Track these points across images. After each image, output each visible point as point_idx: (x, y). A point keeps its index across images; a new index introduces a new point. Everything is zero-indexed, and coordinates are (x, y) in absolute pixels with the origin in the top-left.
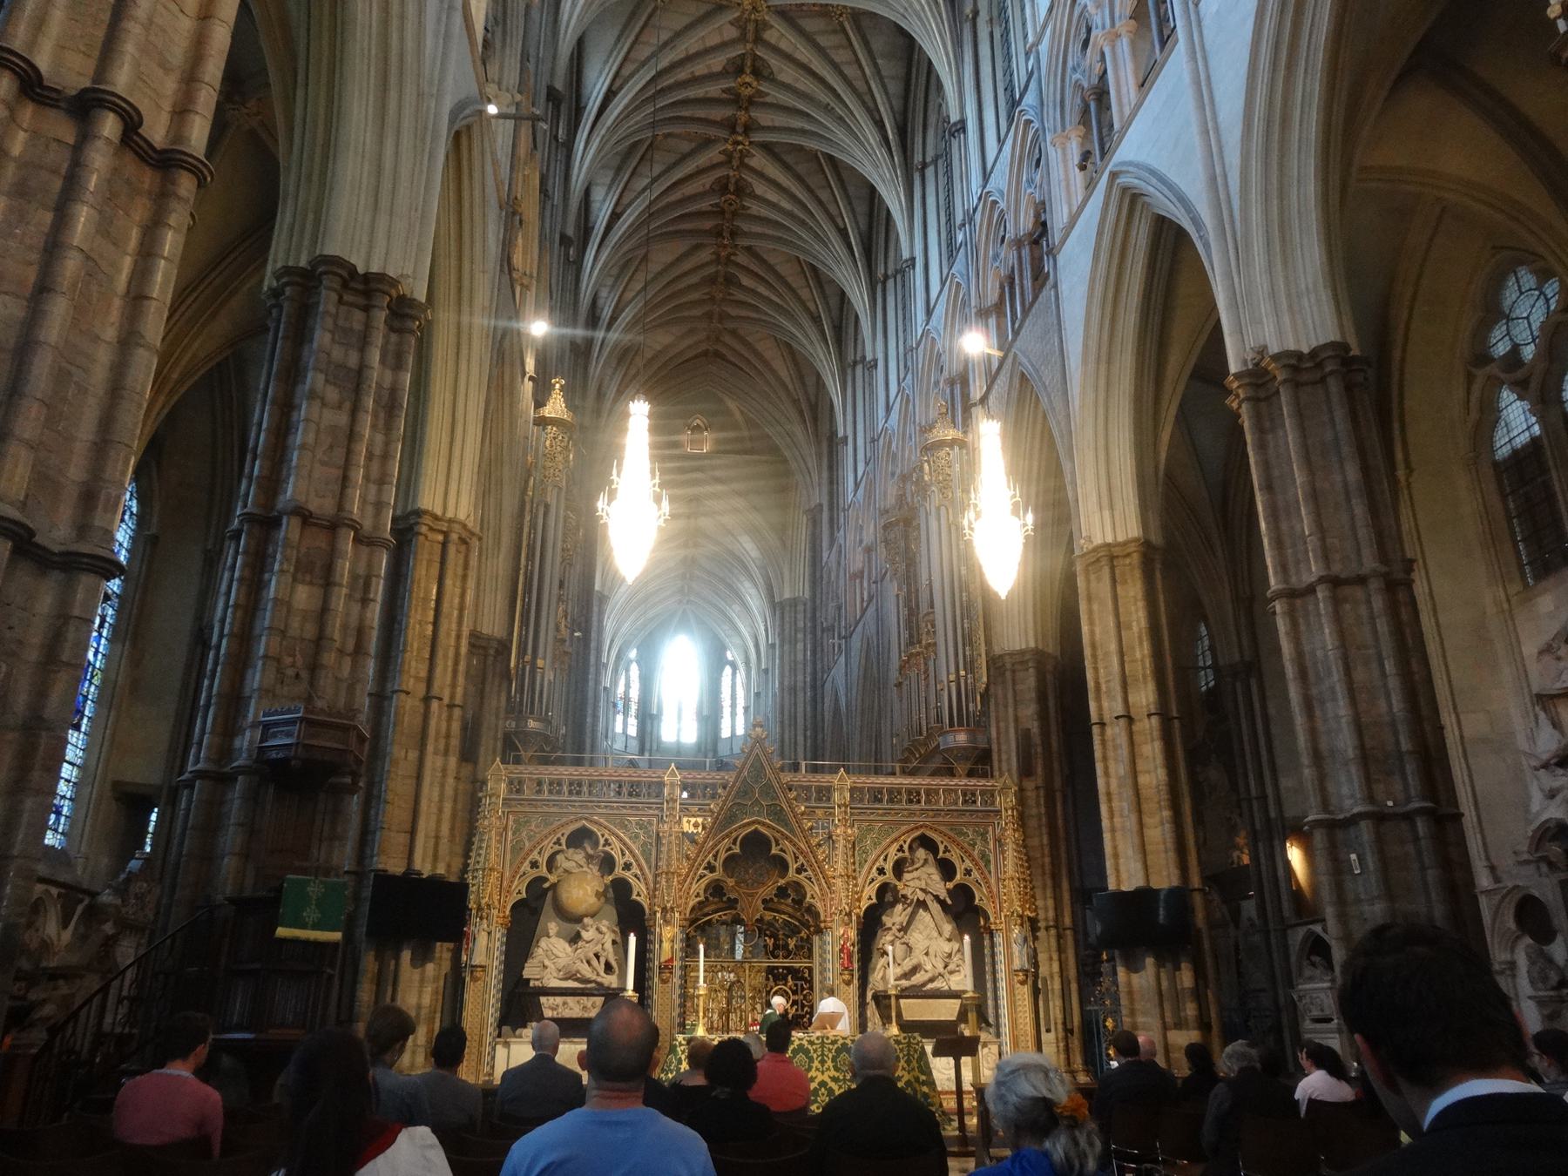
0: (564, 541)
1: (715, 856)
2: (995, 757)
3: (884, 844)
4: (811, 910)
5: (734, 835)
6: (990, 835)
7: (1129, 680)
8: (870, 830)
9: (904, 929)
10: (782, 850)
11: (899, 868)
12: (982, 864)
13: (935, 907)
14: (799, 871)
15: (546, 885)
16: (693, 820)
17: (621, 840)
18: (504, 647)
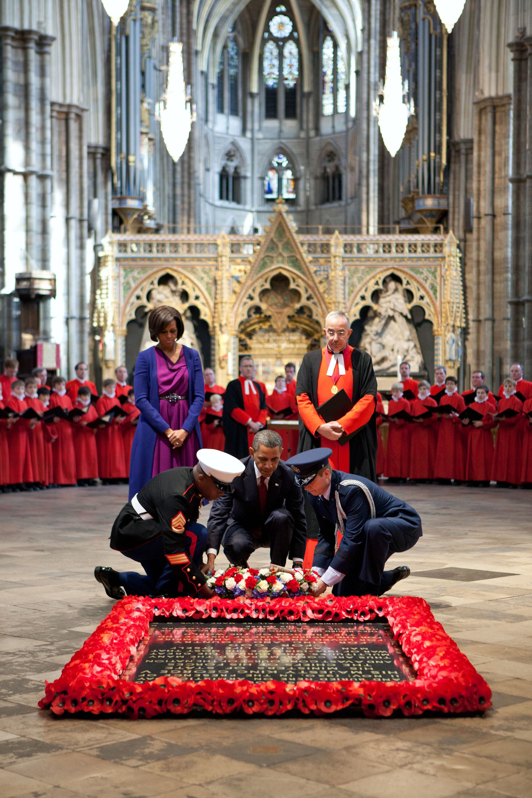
0: (143, 38)
1: (254, 290)
2: (451, 216)
3: (365, 280)
4: (318, 323)
5: (265, 277)
6: (438, 274)
7: (496, 190)
8: (356, 271)
9: (379, 334)
10: (298, 286)
11: (376, 295)
12: (431, 292)
13: (401, 320)
14: (309, 298)
15: (147, 310)
16: (238, 267)
17: (192, 282)
18: (107, 151)
